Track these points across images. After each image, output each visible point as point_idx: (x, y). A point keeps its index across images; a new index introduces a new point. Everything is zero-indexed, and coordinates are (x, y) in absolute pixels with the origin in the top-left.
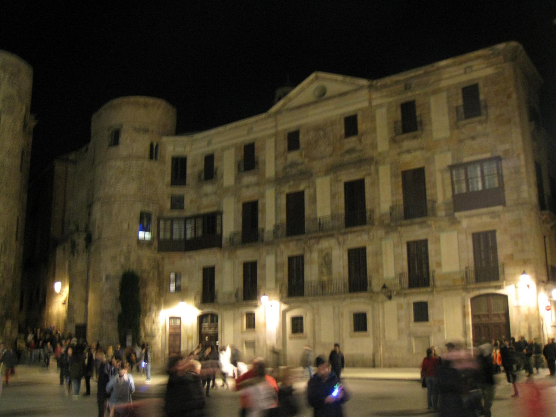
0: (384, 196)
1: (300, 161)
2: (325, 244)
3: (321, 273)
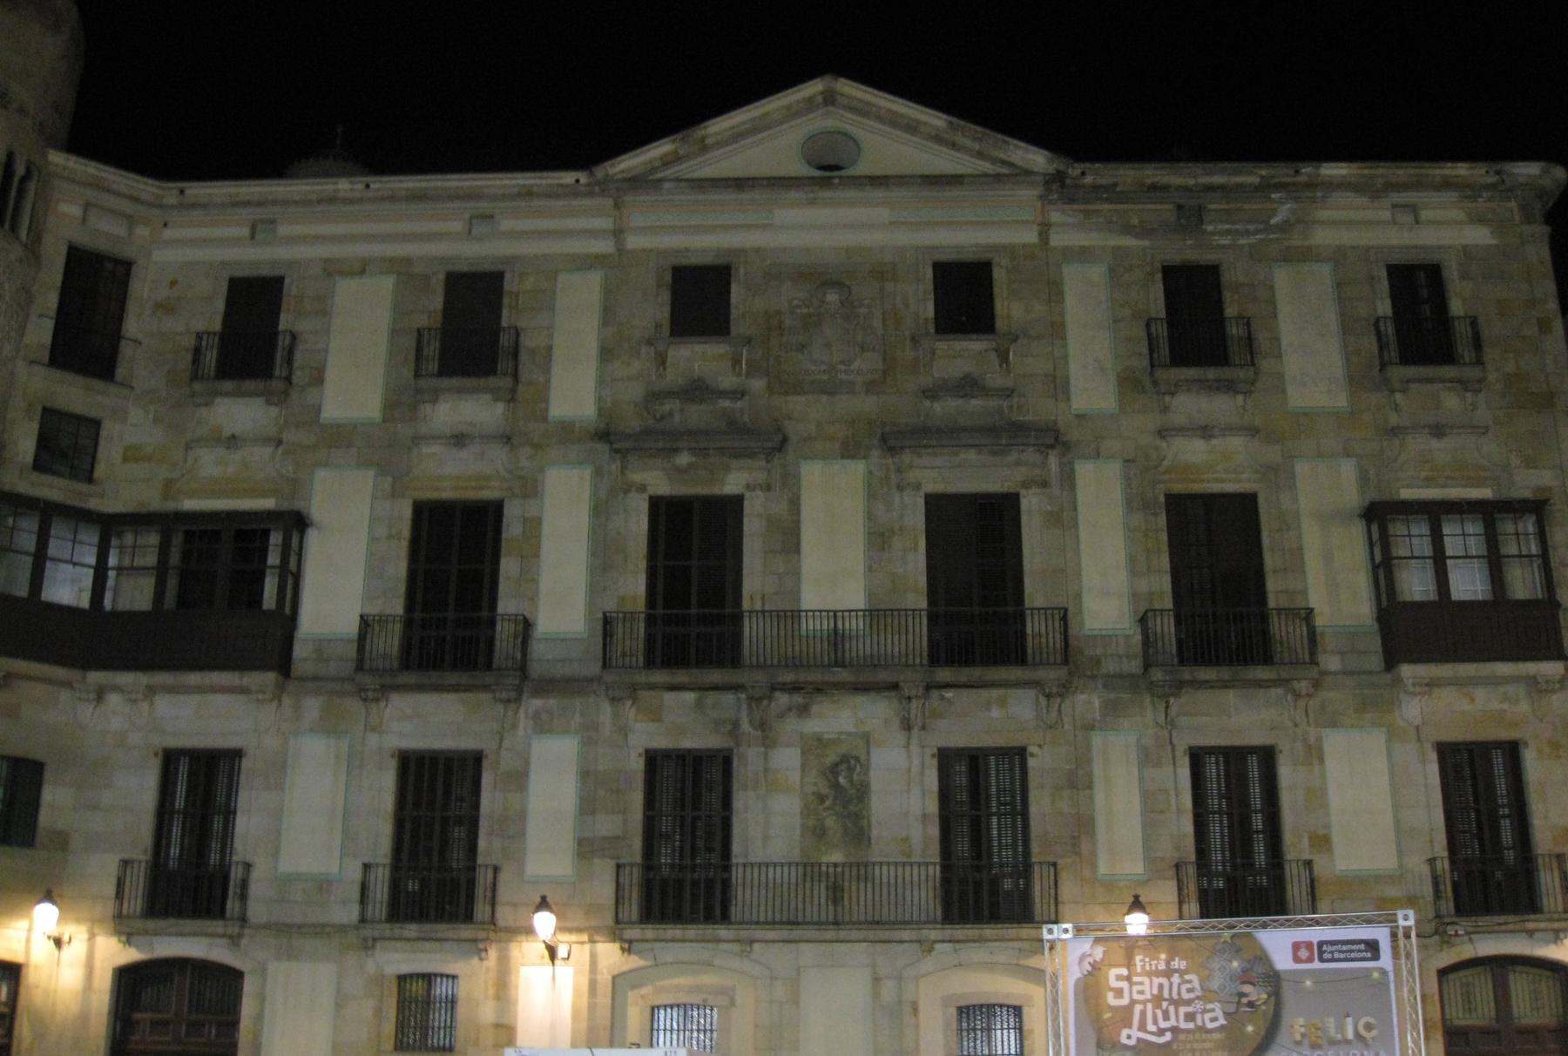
0: (1099, 568)
1: (727, 381)
2: (839, 718)
3: (819, 832)
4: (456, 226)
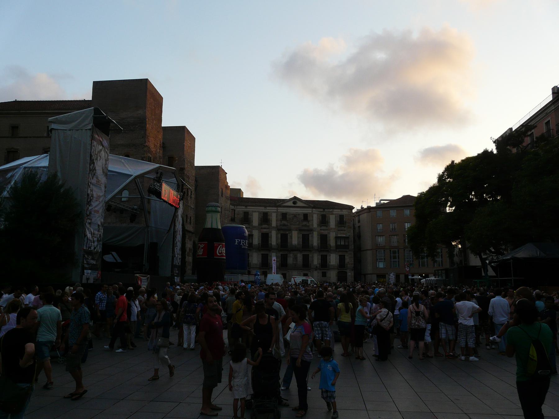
0: (315, 241)
4: (263, 208)
